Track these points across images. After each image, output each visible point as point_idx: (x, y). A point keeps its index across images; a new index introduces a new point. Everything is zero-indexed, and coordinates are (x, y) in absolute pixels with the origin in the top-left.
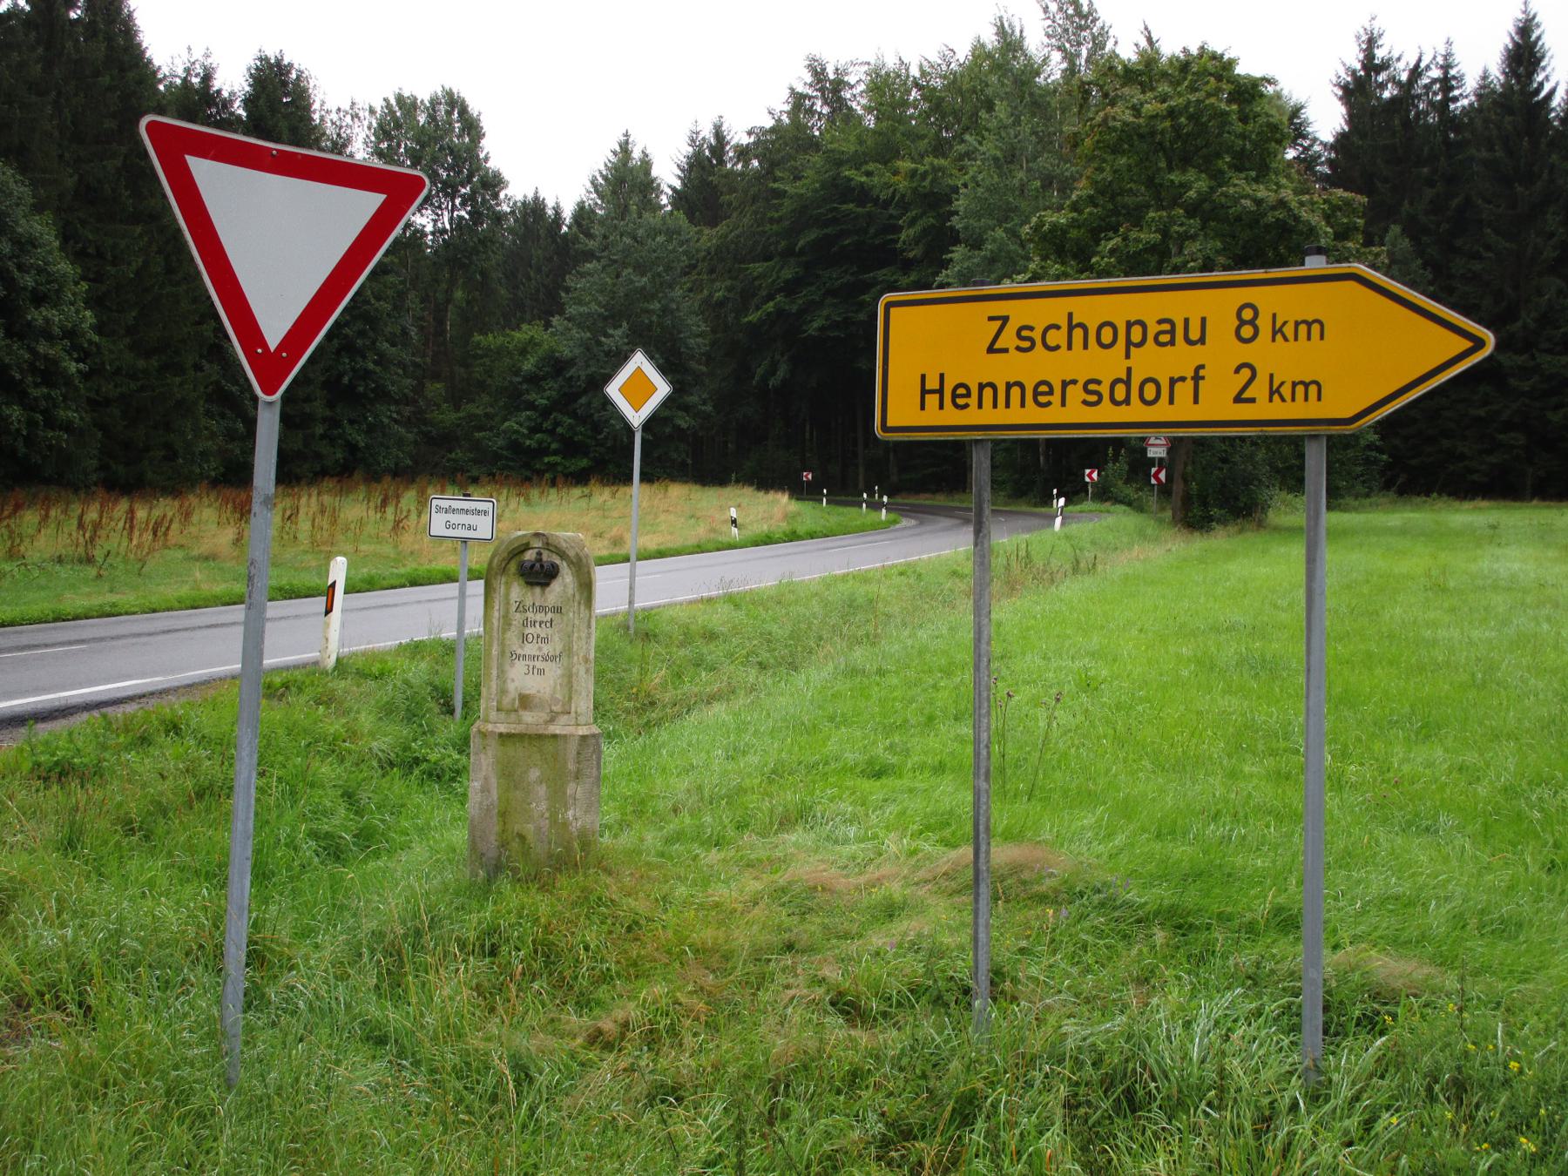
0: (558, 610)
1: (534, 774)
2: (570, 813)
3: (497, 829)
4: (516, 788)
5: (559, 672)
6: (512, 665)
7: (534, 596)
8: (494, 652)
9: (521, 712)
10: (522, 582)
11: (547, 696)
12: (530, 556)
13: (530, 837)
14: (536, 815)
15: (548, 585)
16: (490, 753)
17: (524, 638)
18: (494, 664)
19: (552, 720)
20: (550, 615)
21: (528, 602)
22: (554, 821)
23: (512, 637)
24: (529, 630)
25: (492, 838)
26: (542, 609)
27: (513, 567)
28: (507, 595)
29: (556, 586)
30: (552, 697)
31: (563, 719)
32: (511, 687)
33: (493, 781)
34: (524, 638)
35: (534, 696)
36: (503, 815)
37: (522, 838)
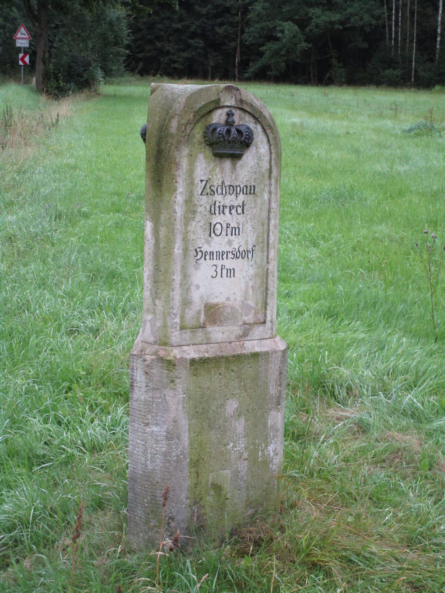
0: (250, 190)
1: (232, 406)
2: (271, 448)
3: (187, 483)
4: (210, 427)
5: (252, 271)
6: (197, 266)
7: (223, 173)
8: (178, 250)
9: (210, 329)
10: (208, 152)
11: (237, 305)
12: (218, 117)
13: (227, 487)
14: (233, 457)
15: (239, 157)
16: (180, 387)
17: (211, 229)
18: (177, 267)
19: (245, 335)
20: (241, 197)
21: (216, 182)
22: (253, 459)
23: (197, 227)
24: (217, 219)
25: (183, 495)
26: (233, 189)
27: (198, 133)
28: (191, 172)
29: (249, 158)
30: (244, 304)
31: (258, 331)
32: (196, 296)
33: (184, 423)
34: (211, 229)
35: (224, 307)
36: (195, 464)
37: (217, 488)
